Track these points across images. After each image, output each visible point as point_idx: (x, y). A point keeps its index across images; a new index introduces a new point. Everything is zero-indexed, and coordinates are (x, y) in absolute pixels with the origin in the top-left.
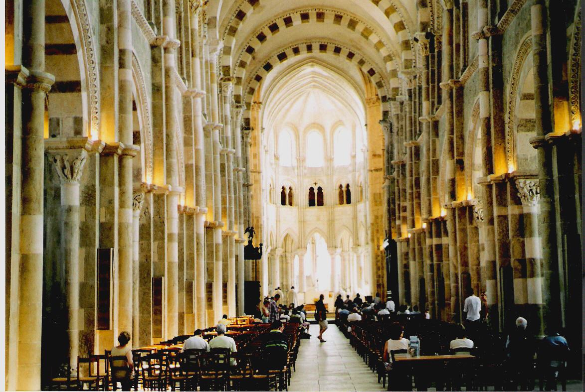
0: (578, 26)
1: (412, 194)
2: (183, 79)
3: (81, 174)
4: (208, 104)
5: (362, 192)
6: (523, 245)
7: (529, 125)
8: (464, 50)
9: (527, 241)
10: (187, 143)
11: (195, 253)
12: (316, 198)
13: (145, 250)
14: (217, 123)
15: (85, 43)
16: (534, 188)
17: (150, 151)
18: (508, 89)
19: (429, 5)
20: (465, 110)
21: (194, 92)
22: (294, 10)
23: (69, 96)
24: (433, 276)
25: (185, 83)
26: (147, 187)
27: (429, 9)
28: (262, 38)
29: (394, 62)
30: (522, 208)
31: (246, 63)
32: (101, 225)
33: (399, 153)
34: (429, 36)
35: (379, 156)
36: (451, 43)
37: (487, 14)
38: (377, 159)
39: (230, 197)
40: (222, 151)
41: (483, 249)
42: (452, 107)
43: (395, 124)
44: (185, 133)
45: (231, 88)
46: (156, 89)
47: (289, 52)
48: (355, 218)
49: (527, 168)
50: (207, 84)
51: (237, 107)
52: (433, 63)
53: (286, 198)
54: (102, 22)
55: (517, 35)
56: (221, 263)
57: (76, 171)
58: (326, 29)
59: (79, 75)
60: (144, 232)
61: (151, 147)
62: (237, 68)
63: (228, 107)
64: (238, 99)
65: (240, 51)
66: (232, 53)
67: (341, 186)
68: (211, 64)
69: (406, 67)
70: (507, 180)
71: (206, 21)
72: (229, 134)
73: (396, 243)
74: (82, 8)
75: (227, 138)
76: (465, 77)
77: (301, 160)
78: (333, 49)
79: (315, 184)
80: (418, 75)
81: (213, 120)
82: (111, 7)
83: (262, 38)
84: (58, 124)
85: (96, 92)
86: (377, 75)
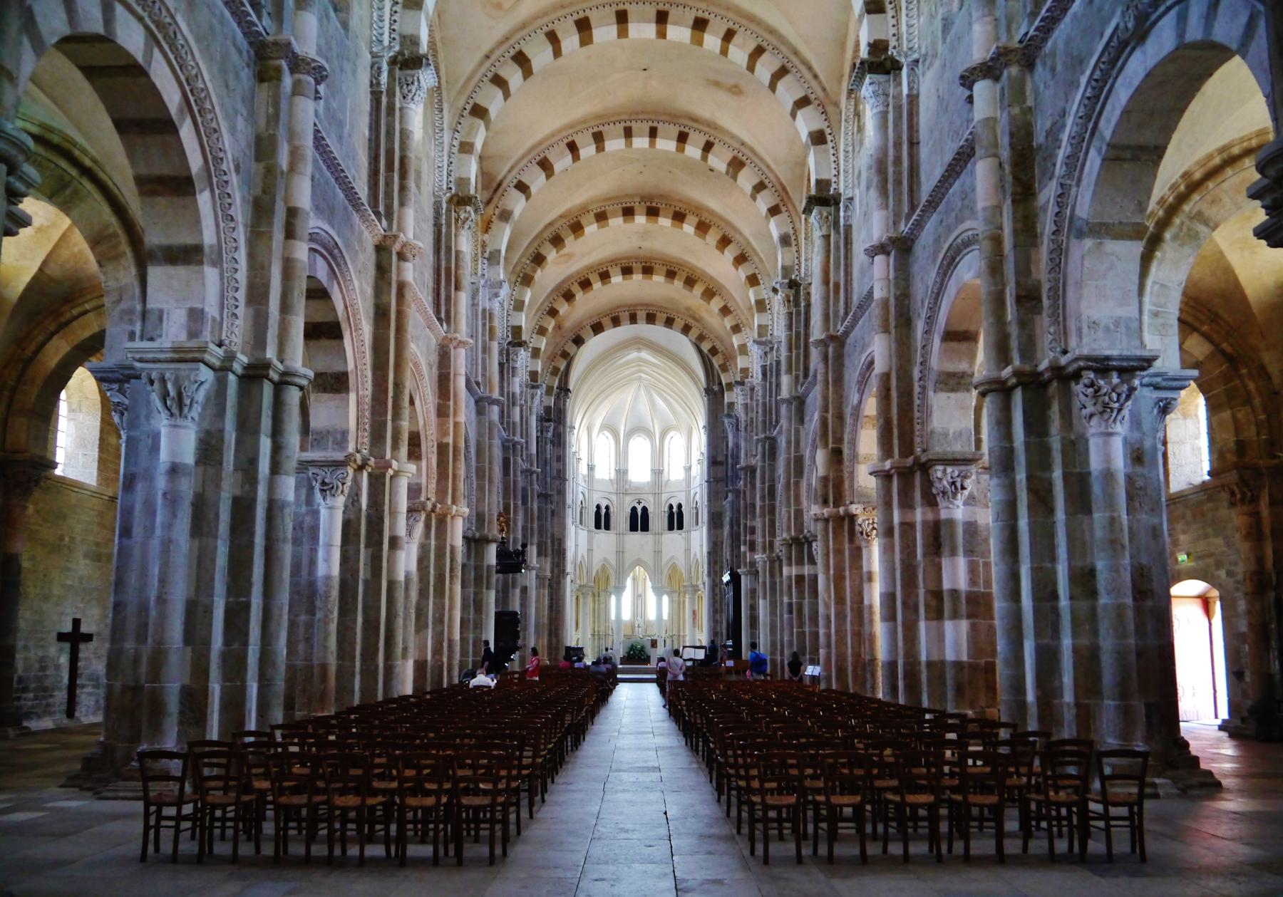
0: (1063, 181)
1: (762, 507)
2: (439, 319)
3: (200, 410)
4: (484, 368)
5: (697, 514)
6: (939, 568)
7: (952, 382)
8: (846, 291)
9: (945, 562)
10: (442, 412)
11: (447, 575)
12: (639, 521)
13: (348, 560)
14: (496, 395)
15: (218, 182)
16: (959, 480)
17: (366, 407)
18: (920, 327)
19: (794, 243)
20: (846, 377)
21: (456, 339)
22: (613, 261)
23: (181, 271)
24: (791, 620)
25: (442, 325)
26: (355, 461)
27: (794, 249)
28: (569, 296)
29: (743, 333)
30: (939, 511)
31: (547, 329)
32: (236, 501)
33: (746, 455)
34: (793, 285)
35: (721, 463)
36: (826, 282)
37: (887, 219)
38: (721, 469)
39: (515, 505)
40: (507, 441)
41: (870, 579)
42: (827, 373)
43: (742, 417)
44: (439, 397)
45: (523, 359)
46: (381, 314)
47: (606, 321)
48: (688, 550)
49: (948, 449)
50: (484, 342)
51: (533, 387)
52: (798, 322)
53: (602, 520)
54: (258, 158)
55: (937, 241)
56: (493, 594)
57: (188, 402)
58: (656, 288)
59: (201, 234)
60: (349, 528)
61: (368, 400)
62: (534, 336)
63: (518, 383)
64: (534, 375)
65: (540, 313)
66: (525, 308)
67: (671, 507)
68: (490, 314)
69: (760, 335)
70: (916, 468)
71: (486, 255)
72: (518, 419)
73: (739, 577)
74: (209, 116)
75: (514, 423)
76: (847, 327)
77: (621, 473)
78: (664, 320)
79: (639, 503)
80: (776, 346)
81: (491, 391)
82: (274, 135)
83: (569, 296)
84: (161, 319)
85: (236, 270)
86: (720, 355)
